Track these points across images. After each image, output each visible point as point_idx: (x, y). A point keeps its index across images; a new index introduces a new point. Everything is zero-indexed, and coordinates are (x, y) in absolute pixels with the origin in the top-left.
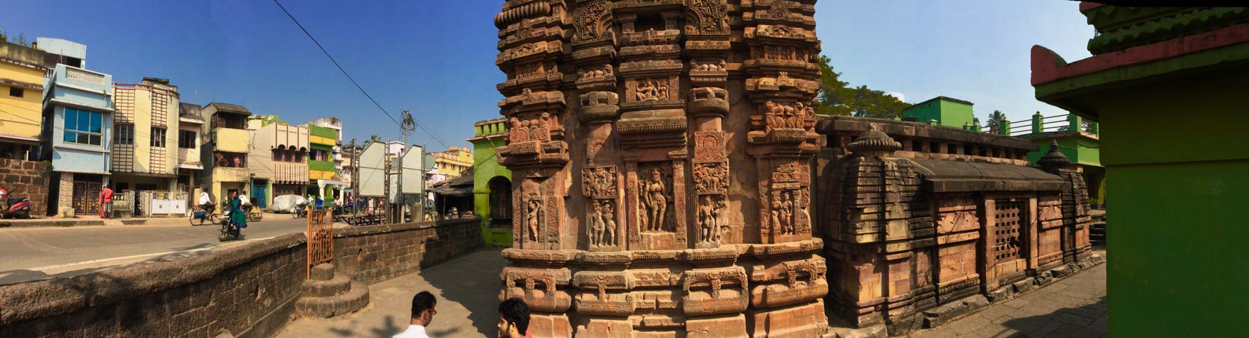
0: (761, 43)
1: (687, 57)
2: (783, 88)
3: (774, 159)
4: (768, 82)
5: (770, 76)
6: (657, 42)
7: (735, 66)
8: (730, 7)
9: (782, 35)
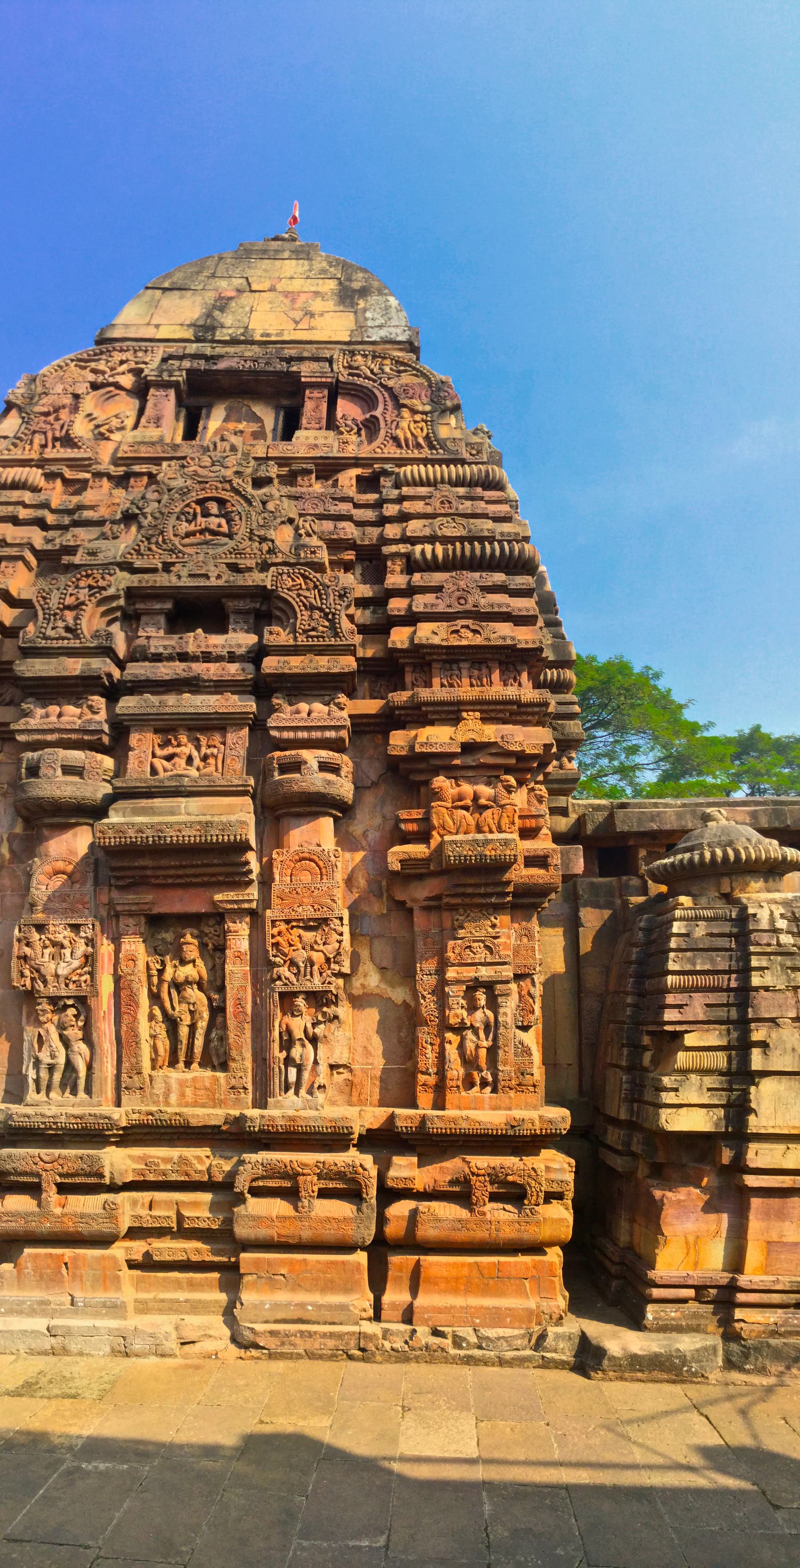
0: (424, 660)
1: (264, 688)
2: (469, 748)
3: (453, 908)
4: (438, 737)
5: (444, 722)
6: (207, 657)
7: (370, 706)
8: (365, 591)
9: (468, 639)
